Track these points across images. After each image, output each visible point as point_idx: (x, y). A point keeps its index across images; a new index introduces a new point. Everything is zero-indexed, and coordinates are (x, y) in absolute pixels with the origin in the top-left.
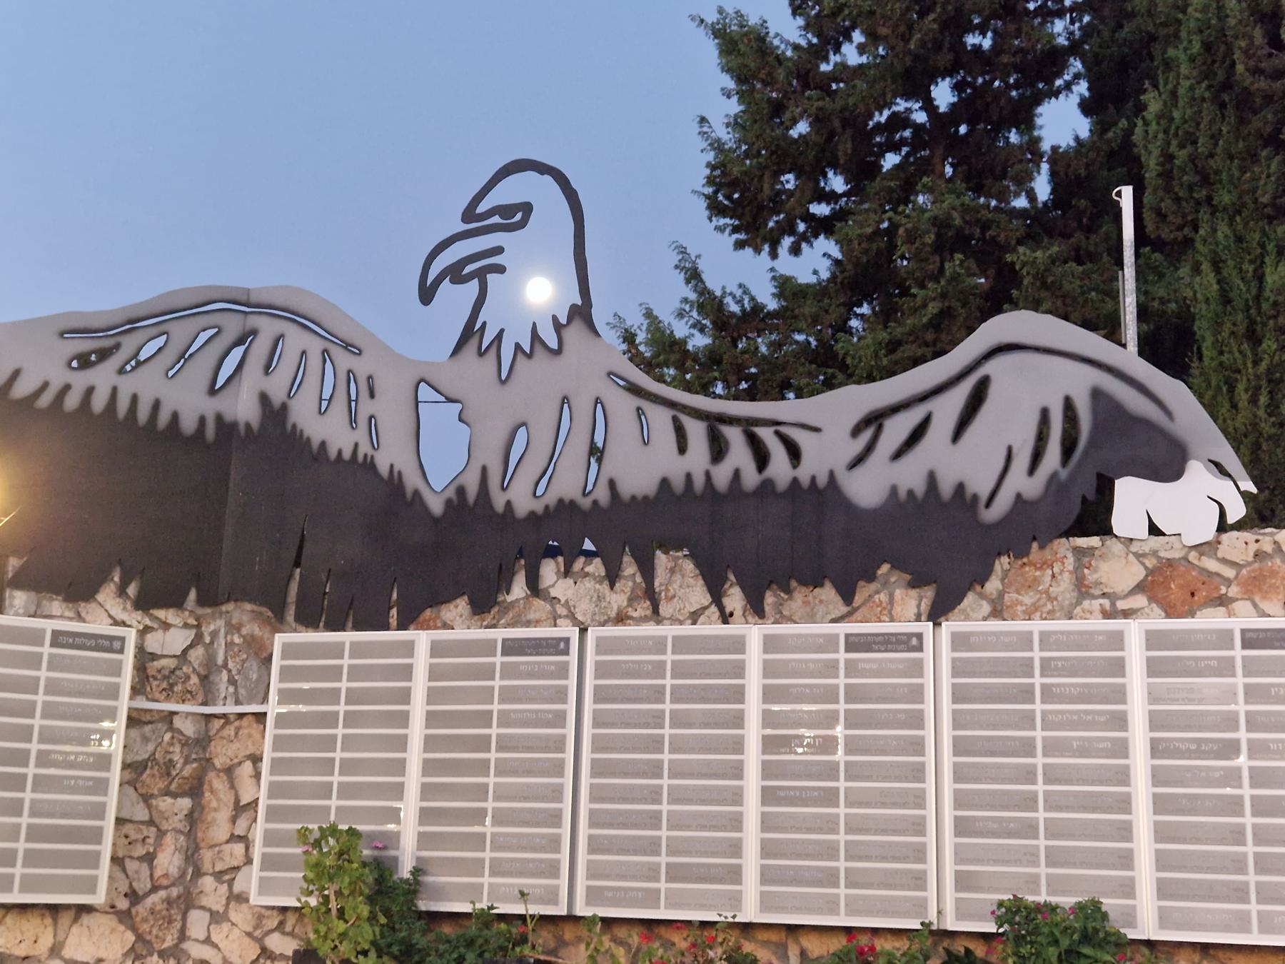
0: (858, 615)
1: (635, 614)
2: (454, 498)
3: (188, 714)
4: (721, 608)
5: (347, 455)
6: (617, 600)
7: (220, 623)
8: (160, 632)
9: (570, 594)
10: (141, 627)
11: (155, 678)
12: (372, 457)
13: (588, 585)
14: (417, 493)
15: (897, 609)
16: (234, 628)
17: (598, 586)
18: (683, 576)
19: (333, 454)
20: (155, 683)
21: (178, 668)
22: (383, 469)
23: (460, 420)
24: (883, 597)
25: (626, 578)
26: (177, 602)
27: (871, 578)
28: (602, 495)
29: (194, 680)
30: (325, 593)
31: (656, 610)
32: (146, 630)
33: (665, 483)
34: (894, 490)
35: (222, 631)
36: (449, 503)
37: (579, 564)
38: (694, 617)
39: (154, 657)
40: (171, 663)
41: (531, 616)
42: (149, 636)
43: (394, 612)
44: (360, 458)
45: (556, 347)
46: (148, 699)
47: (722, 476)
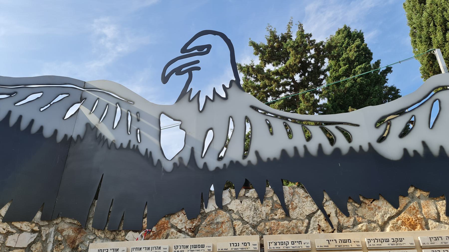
1: (276, 217)
2: (178, 163)
4: (324, 212)
5: (125, 146)
6: (265, 210)
7: (52, 229)
8: (17, 235)
9: (239, 208)
10: (5, 232)
12: (137, 146)
13: (249, 203)
14: (159, 160)
15: (425, 210)
16: (58, 231)
17: (254, 203)
18: (299, 197)
19: (118, 145)
22: (143, 151)
23: (181, 128)
24: (414, 204)
25: (268, 198)
26: (29, 218)
27: (405, 195)
28: (252, 157)
30: (110, 212)
31: (287, 214)
33: (284, 152)
34: (405, 150)
35: (53, 233)
36: (175, 164)
37: (242, 192)
41: (220, 220)
43: (145, 220)
44: (131, 147)
45: (225, 97)
47: (313, 147)
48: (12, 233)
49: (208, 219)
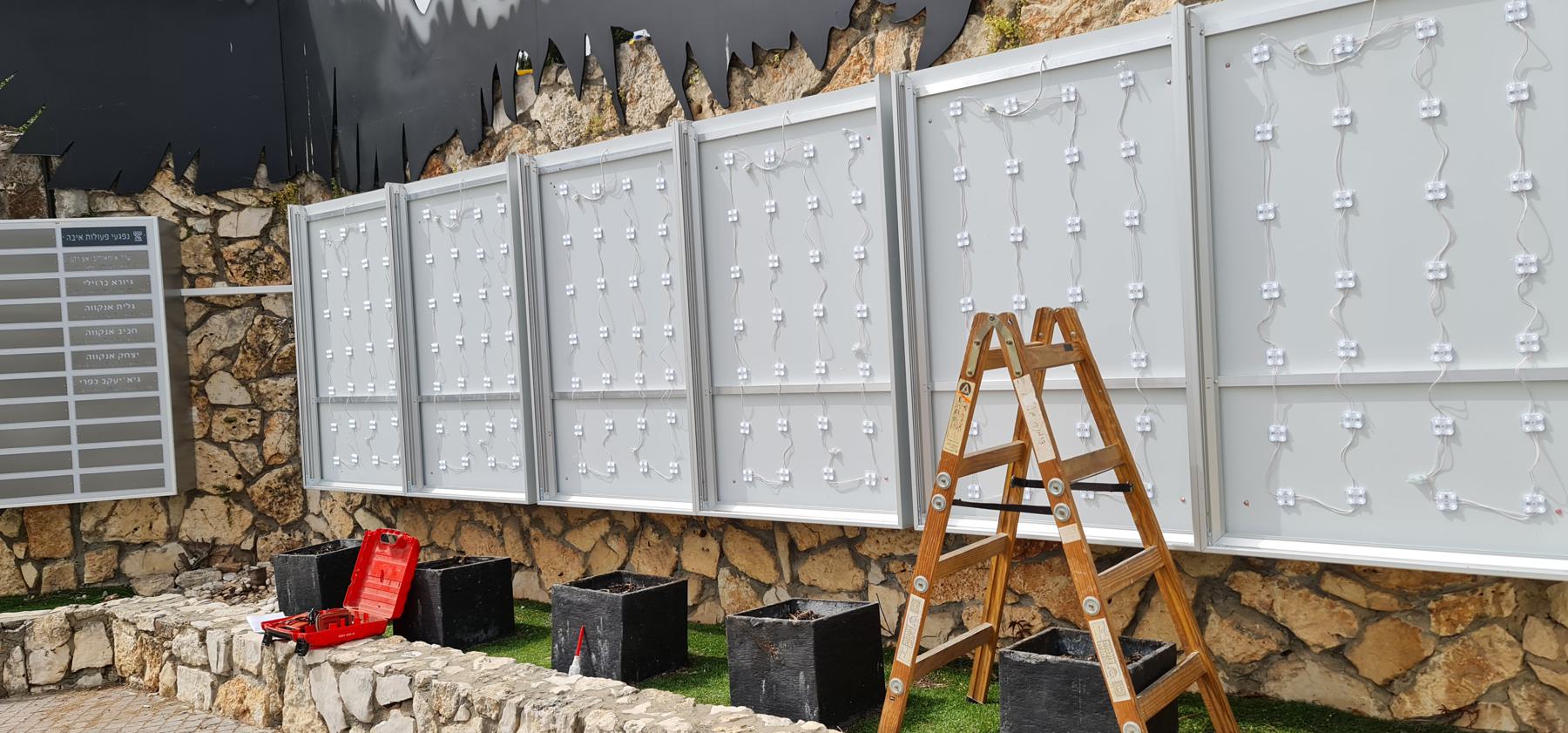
0: (834, 82)
3: (277, 296)
6: (586, 111)
8: (234, 214)
11: (233, 262)
15: (880, 60)
20: (235, 267)
21: (260, 249)
25: (595, 82)
26: (247, 183)
29: (279, 259)
32: (216, 216)
36: (433, 23)
38: (662, 119)
39: (230, 241)
40: (252, 245)
42: (223, 221)
46: (230, 284)
48: (226, 212)
49: (498, 148)
